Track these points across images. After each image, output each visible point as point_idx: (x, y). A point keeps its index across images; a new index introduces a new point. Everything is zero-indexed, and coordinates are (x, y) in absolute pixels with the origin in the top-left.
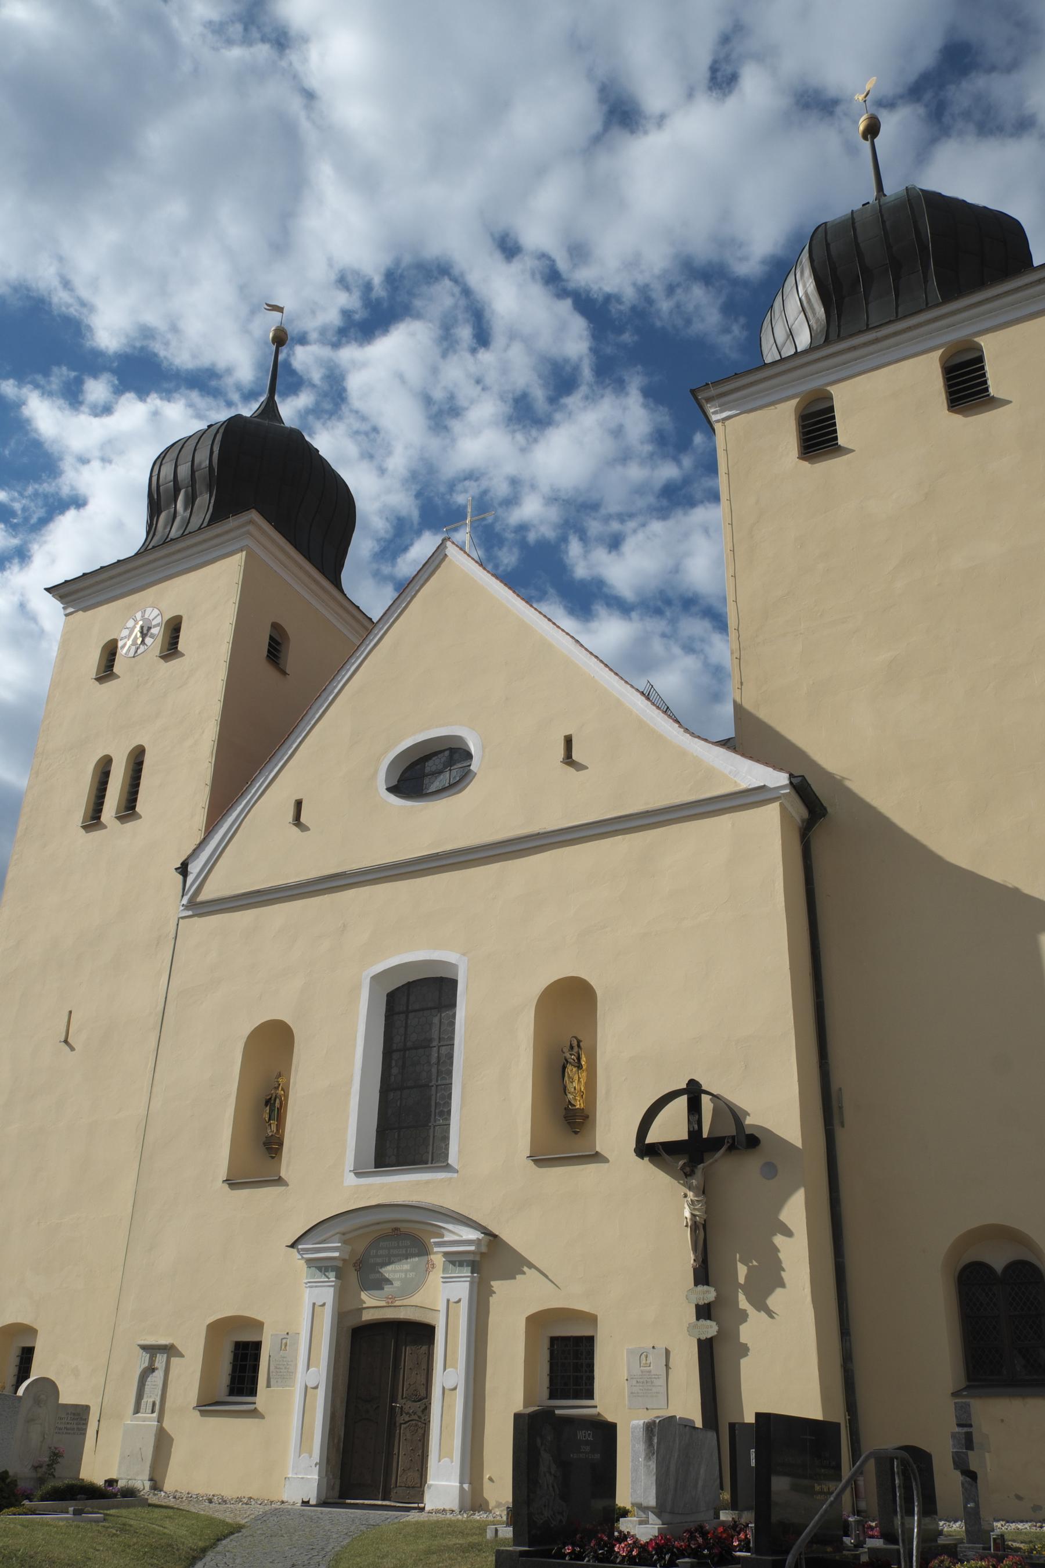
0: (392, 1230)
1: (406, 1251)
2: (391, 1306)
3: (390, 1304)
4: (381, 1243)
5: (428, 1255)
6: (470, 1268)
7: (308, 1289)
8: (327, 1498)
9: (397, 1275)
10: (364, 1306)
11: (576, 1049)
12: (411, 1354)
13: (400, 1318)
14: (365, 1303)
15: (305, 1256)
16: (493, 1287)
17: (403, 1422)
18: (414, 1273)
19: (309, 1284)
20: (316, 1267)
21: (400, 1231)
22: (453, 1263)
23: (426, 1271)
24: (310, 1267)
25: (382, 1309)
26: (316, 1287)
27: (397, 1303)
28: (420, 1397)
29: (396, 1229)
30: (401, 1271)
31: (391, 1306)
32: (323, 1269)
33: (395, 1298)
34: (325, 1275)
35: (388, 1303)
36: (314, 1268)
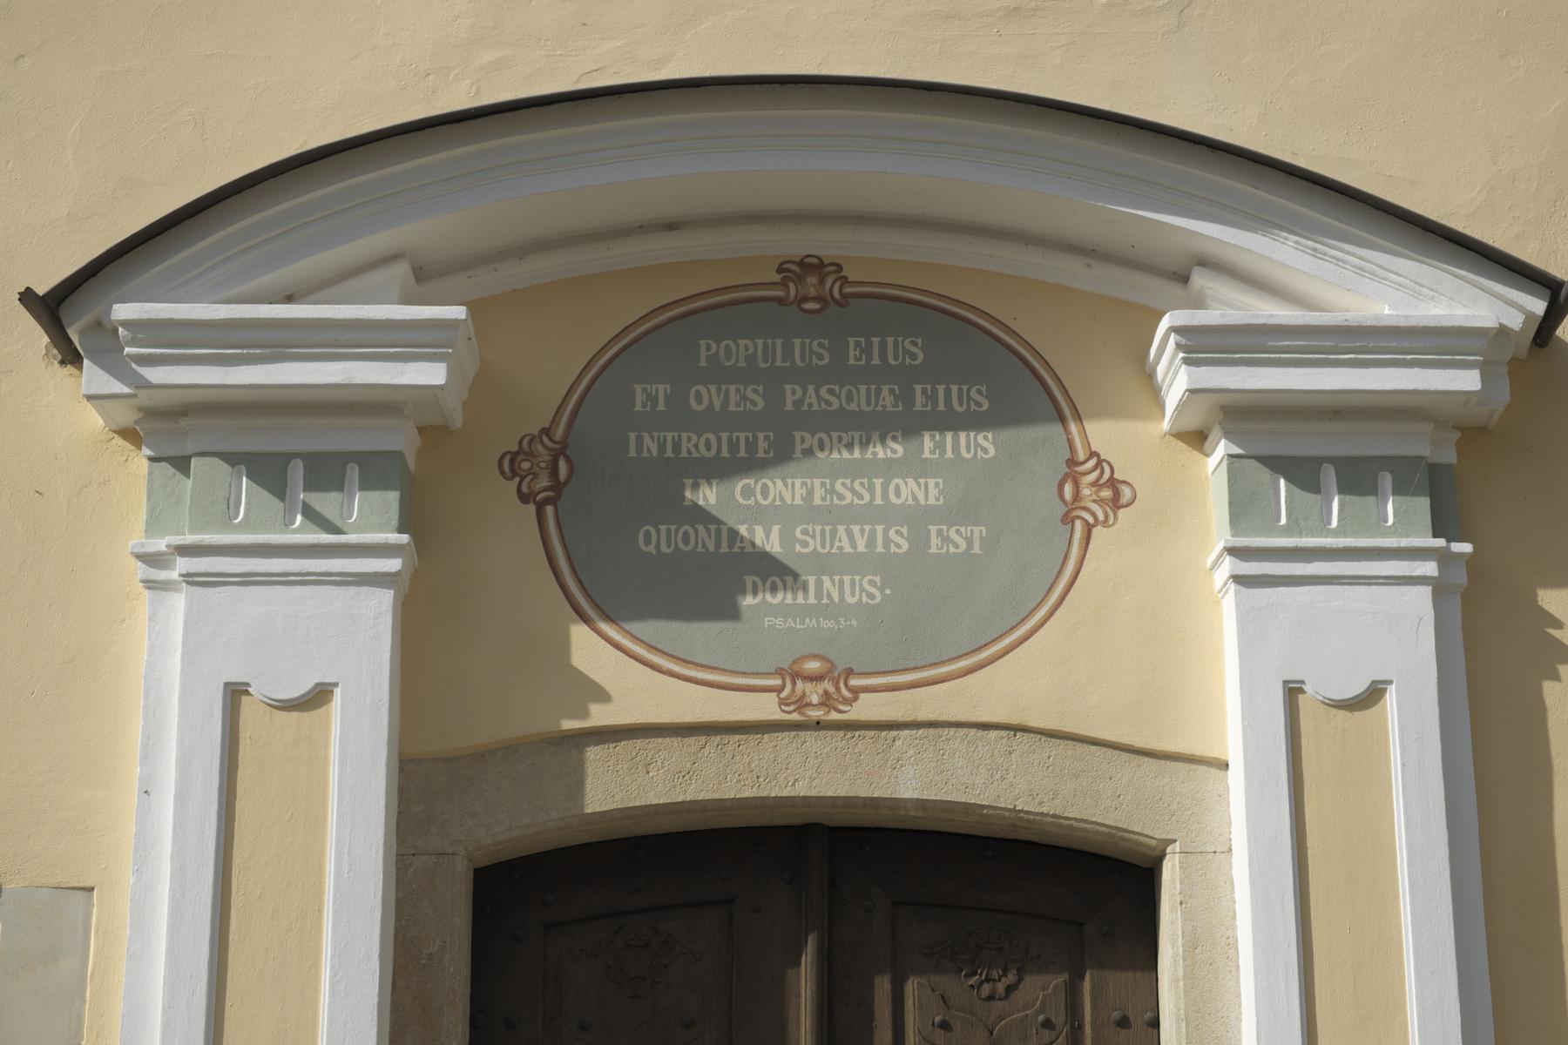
0: (780, 270)
1: (907, 397)
2: (818, 725)
3: (815, 714)
4: (706, 349)
5: (1062, 419)
6: (1422, 504)
7: (178, 603)
9: (852, 540)
10: (600, 716)
12: (945, 1026)
13: (894, 803)
14: (602, 696)
15: (156, 375)
16: (1559, 625)
18: (978, 531)
19: (183, 564)
20: (231, 459)
21: (845, 281)
22: (1303, 472)
23: (1068, 519)
24: (181, 464)
25: (752, 739)
26: (247, 580)
27: (867, 708)
29: (812, 267)
30: (887, 515)
31: (818, 725)
32: (297, 471)
33: (849, 672)
34: (310, 514)
35: (802, 704)
36: (217, 461)
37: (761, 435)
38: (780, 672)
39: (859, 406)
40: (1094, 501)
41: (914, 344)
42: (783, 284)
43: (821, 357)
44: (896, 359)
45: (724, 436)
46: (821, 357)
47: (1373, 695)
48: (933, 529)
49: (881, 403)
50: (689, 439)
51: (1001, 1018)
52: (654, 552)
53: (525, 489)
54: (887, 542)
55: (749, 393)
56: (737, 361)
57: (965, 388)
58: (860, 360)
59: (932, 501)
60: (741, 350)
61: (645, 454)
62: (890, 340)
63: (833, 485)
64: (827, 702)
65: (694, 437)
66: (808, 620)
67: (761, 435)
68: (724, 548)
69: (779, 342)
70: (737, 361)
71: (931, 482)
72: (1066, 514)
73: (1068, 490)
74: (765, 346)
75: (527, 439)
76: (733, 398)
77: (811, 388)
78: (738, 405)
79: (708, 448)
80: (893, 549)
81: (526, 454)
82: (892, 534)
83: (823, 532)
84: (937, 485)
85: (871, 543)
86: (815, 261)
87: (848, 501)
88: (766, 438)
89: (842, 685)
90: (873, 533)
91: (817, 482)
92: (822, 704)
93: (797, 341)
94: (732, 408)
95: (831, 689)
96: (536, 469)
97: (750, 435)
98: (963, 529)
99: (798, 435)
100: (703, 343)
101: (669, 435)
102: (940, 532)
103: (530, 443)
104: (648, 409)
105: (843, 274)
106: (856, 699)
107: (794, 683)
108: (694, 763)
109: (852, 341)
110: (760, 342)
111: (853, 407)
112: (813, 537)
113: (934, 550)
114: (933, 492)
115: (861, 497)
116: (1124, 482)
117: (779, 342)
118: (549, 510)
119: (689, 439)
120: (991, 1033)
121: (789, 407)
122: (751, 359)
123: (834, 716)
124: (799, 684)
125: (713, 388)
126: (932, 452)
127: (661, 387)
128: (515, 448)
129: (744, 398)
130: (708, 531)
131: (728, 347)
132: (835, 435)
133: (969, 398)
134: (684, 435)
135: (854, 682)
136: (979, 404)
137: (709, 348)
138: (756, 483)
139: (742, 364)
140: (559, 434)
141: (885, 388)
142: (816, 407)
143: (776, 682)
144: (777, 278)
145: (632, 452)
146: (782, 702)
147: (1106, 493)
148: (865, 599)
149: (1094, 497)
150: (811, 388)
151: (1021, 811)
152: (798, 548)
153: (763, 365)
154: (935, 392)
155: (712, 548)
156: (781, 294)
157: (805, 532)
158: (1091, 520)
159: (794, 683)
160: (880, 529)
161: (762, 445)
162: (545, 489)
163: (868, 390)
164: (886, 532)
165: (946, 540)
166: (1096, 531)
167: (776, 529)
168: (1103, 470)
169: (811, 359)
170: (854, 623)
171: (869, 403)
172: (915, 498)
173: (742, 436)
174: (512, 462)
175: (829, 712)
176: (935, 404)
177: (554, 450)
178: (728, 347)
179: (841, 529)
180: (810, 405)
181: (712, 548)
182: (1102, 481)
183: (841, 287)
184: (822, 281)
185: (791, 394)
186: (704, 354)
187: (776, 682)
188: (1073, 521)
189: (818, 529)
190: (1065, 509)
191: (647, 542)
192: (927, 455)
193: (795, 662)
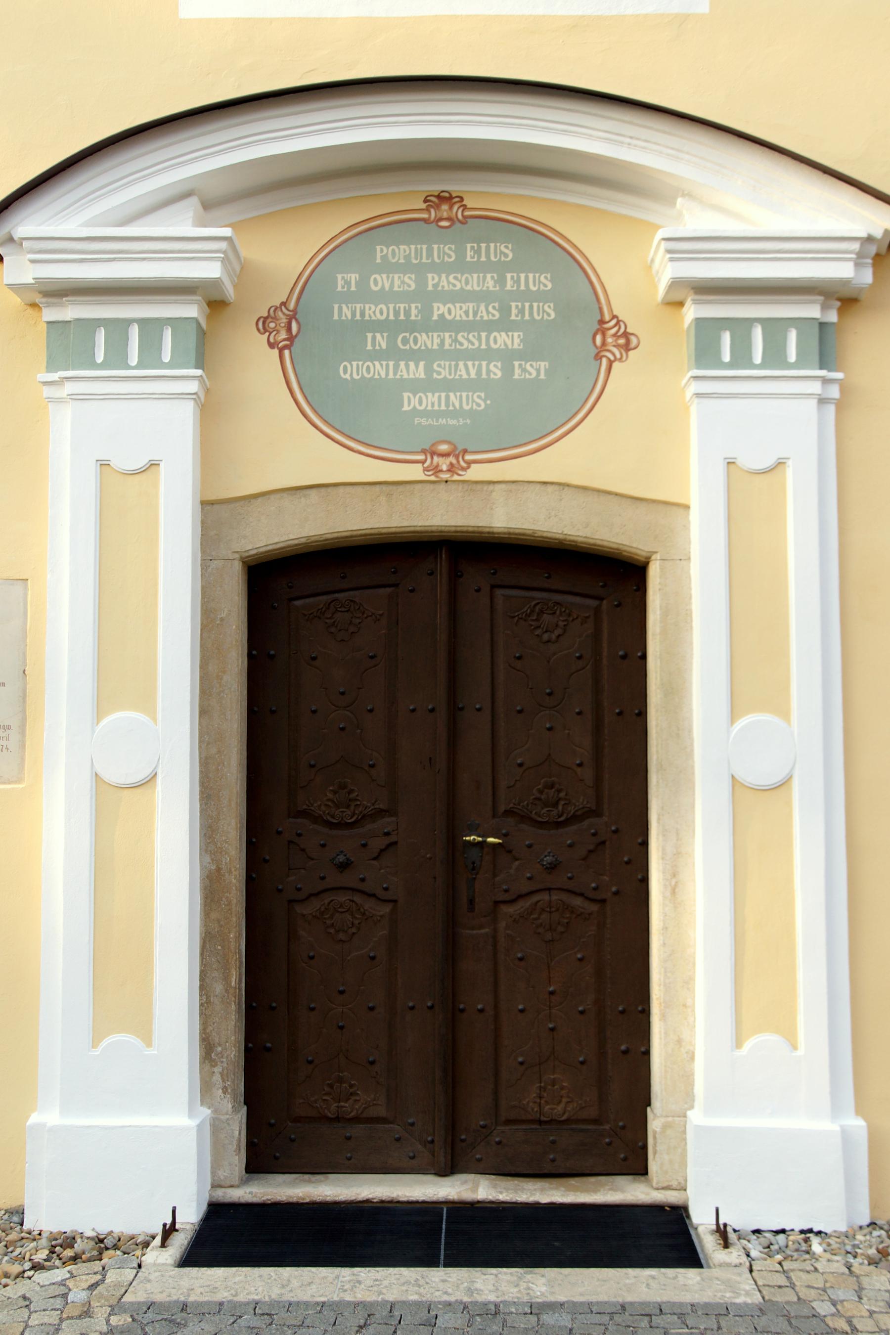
0: (425, 201)
1: (501, 281)
4: (381, 251)
8: (215, 1186)
17: (507, 897)
18: (543, 365)
21: (465, 207)
23: (598, 357)
27: (476, 473)
28: (571, 809)
30: (488, 355)
33: (465, 451)
35: (437, 470)
37: (413, 306)
38: (424, 451)
39: (472, 287)
40: (614, 346)
41: (507, 247)
42: (427, 210)
43: (450, 257)
44: (496, 257)
45: (391, 306)
46: (450, 257)
47: (780, 464)
48: (516, 364)
49: (486, 285)
50: (370, 309)
51: (554, 654)
52: (349, 378)
53: (272, 340)
54: (489, 372)
55: (406, 280)
56: (399, 259)
57: (537, 275)
58: (473, 258)
59: (516, 346)
60: (401, 252)
61: (344, 318)
62: (492, 245)
63: (456, 337)
64: (451, 469)
65: (373, 307)
66: (440, 420)
67: (413, 306)
68: (391, 376)
69: (424, 247)
70: (399, 259)
71: (516, 334)
72: (597, 354)
73: (599, 339)
74: (416, 249)
75: (272, 309)
76: (397, 282)
77: (444, 276)
78: (399, 287)
79: (381, 313)
80: (492, 376)
81: (271, 318)
82: (492, 367)
83: (450, 366)
84: (519, 336)
85: (479, 373)
86: (447, 195)
87: (465, 347)
88: (417, 307)
89: (461, 459)
90: (480, 366)
91: (447, 335)
92: (449, 471)
93: (435, 247)
94: (396, 289)
95: (454, 461)
96: (278, 328)
97: (407, 305)
98: (534, 364)
99: (435, 305)
100: (378, 248)
101: (358, 306)
102: (520, 365)
103: (275, 311)
104: (345, 289)
105: (464, 203)
106: (469, 467)
107: (432, 458)
108: (374, 506)
109: (469, 246)
110: (413, 247)
111: (469, 288)
112: (444, 369)
113: (516, 377)
114: (517, 341)
115: (473, 344)
116: (632, 334)
117: (424, 247)
118: (287, 352)
119: (370, 309)
120: (549, 662)
121: (430, 288)
122: (407, 257)
123: (456, 477)
124: (435, 458)
125: (384, 276)
126: (517, 316)
127: (353, 276)
128: (266, 315)
129: (403, 282)
130: (381, 365)
131: (393, 250)
132: (458, 305)
133: (540, 282)
134: (367, 306)
135: (468, 457)
136: (545, 286)
137: (382, 251)
138: (410, 335)
139: (402, 261)
140: (292, 306)
141: (489, 276)
142: (446, 288)
143: (421, 457)
144: (424, 206)
145: (336, 317)
146: (426, 469)
147: (622, 341)
148: (475, 407)
149: (614, 344)
150: (444, 276)
151: (566, 534)
152: (435, 375)
153: (414, 261)
154: (519, 277)
155: (383, 376)
156: (425, 216)
157: (439, 366)
158: (612, 358)
159: (432, 458)
160: (484, 363)
161: (414, 312)
162: (284, 340)
163: (479, 277)
164: (488, 365)
165: (524, 370)
166: (616, 365)
167: (422, 364)
168: (620, 328)
169: (444, 257)
170: (468, 421)
171: (478, 285)
172: (506, 344)
173: (402, 306)
174: (264, 323)
175: (452, 476)
176: (519, 286)
177: (288, 315)
178: (393, 250)
179: (461, 364)
180: (443, 287)
181: (383, 376)
182: (620, 334)
183: (463, 211)
184: (451, 208)
185: (432, 280)
186: (379, 255)
187: (421, 457)
188: (601, 359)
189: (447, 363)
190: (597, 351)
191: (345, 372)
192: (513, 317)
193: (433, 445)
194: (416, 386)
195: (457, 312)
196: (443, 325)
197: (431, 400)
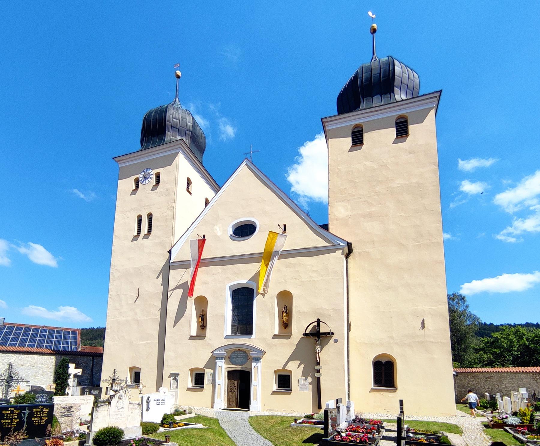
11: (286, 309)
29: (239, 349)
60: (236, 353)
194: (237, 361)
195: (240, 356)
196: (239, 357)
197: (238, 362)
